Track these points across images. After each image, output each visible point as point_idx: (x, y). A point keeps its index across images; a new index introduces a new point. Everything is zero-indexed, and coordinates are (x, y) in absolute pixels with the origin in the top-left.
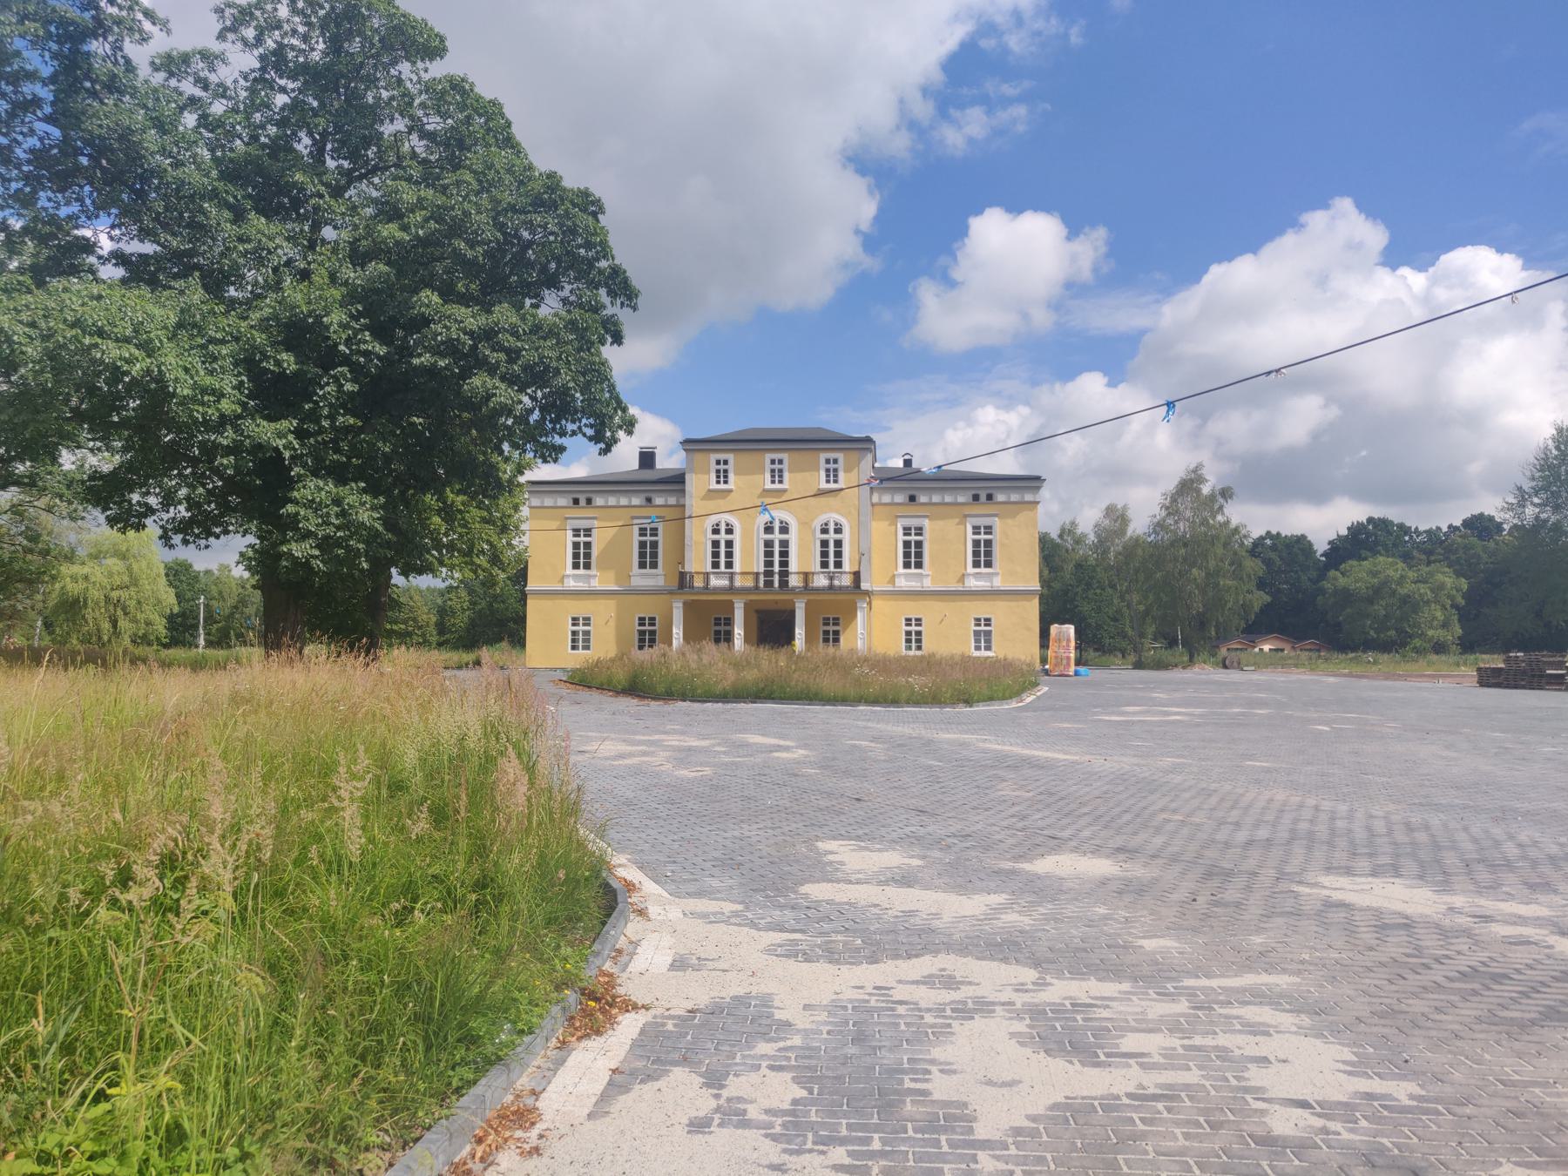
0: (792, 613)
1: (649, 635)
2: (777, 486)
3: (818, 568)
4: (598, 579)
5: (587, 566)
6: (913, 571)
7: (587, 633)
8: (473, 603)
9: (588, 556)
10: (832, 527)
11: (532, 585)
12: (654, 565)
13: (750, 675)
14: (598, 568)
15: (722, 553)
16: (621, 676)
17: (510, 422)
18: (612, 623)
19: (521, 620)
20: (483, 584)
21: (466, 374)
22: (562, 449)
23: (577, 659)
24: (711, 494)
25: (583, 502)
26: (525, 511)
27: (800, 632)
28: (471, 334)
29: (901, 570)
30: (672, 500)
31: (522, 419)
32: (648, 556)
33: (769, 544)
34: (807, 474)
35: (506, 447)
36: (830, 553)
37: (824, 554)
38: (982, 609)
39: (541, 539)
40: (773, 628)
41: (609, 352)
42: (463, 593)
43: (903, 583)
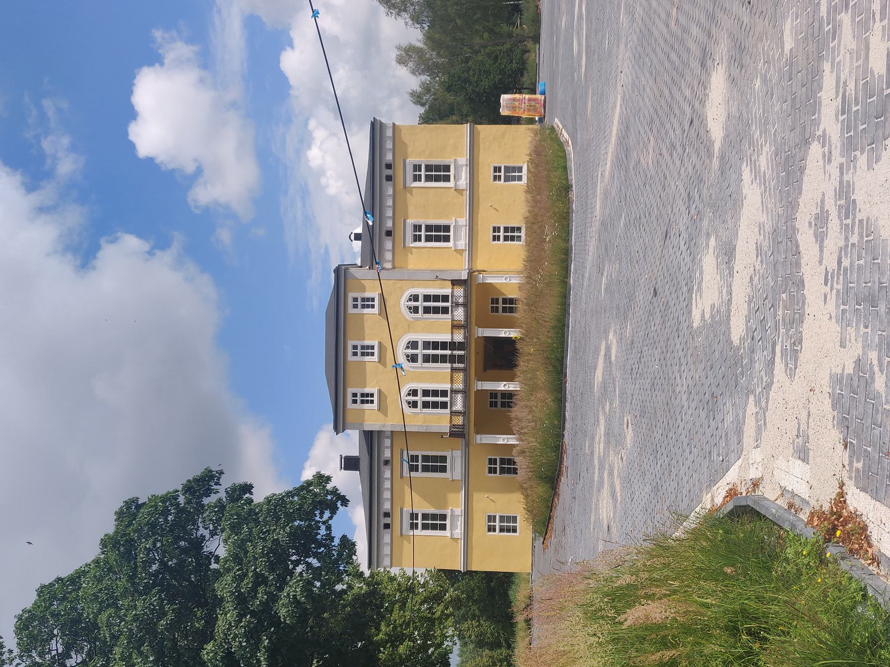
0: (488, 339)
1: (505, 465)
2: (376, 351)
3: (449, 316)
4: (455, 508)
5: (443, 517)
6: (451, 234)
7: (502, 519)
8: (474, 617)
9: (434, 517)
12: (444, 459)
13: (542, 377)
14: (445, 508)
15: (434, 400)
16: (541, 490)
17: (318, 584)
18: (493, 496)
19: (489, 576)
20: (459, 609)
21: (275, 620)
22: (344, 538)
23: (525, 528)
24: (382, 408)
25: (388, 520)
26: (395, 571)
27: (503, 333)
28: (241, 616)
29: (451, 244)
30: (387, 442)
31: (316, 573)
32: (436, 464)
33: (427, 359)
34: (366, 324)
35: (339, 587)
36: (434, 305)
37: (436, 310)
38: (486, 174)
39: (420, 557)
40: (500, 357)
41: (259, 496)
42: (465, 626)
43: (462, 243)
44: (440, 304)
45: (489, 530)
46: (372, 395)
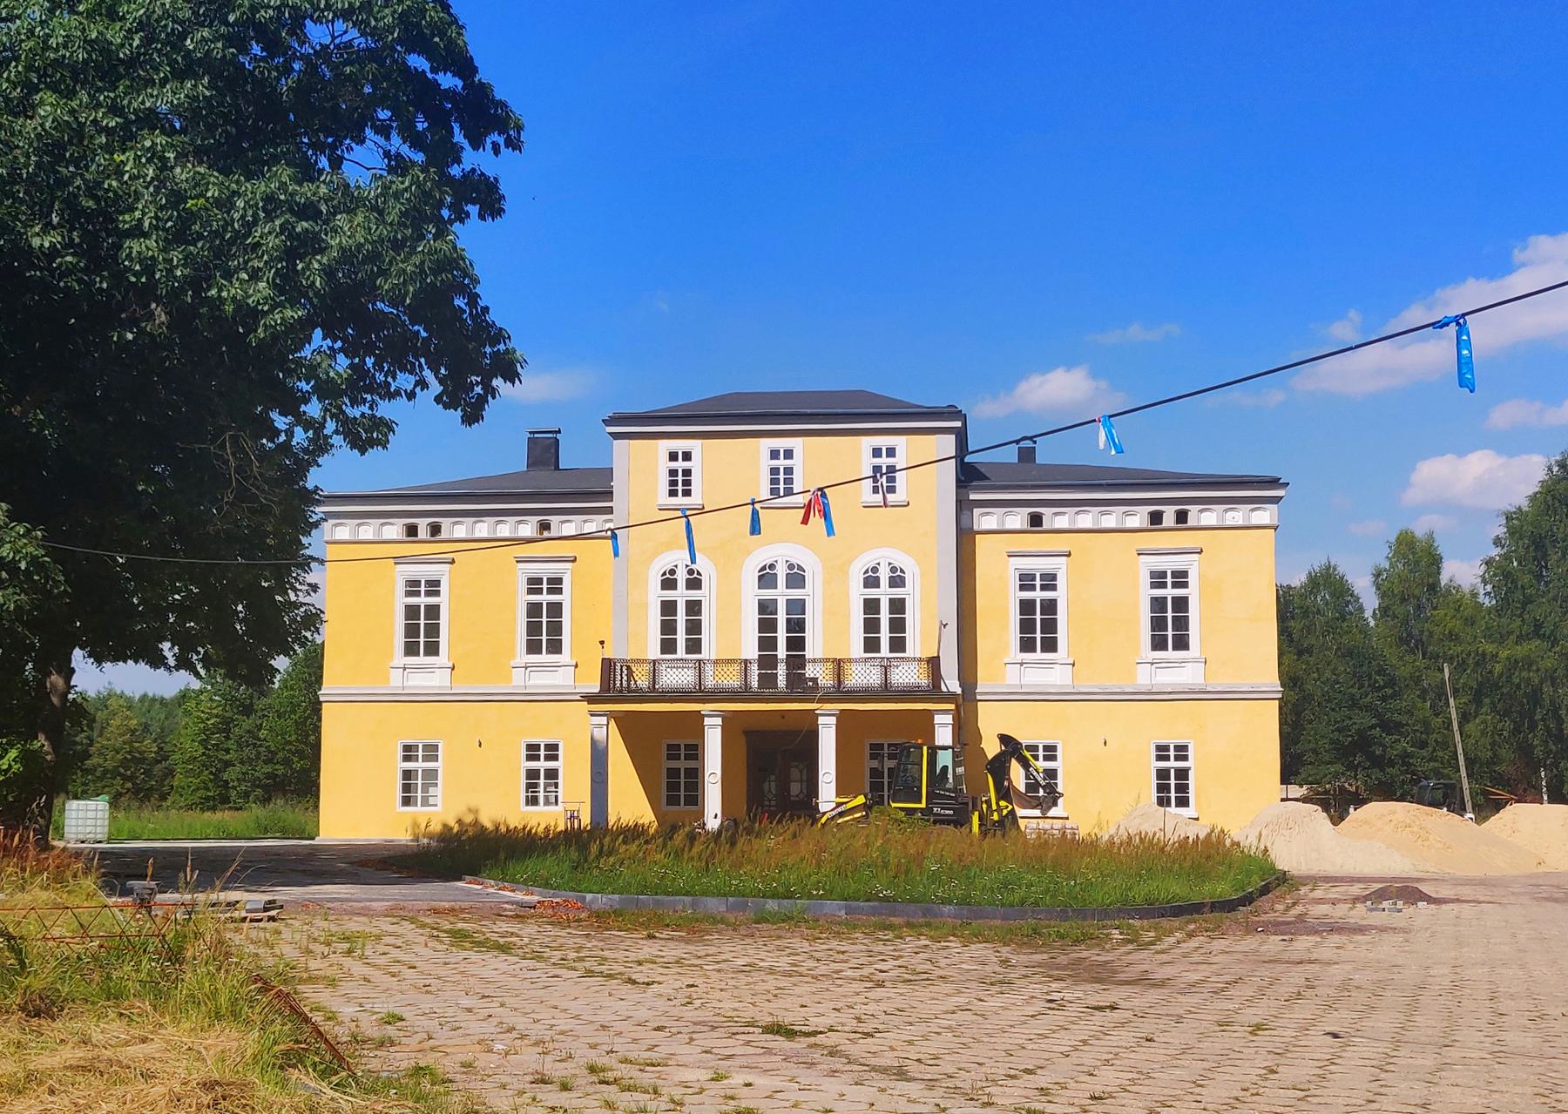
10: (884, 575)
11: (327, 688)
15: (682, 624)
44: (885, 635)
45: (407, 748)
46: (687, 493)
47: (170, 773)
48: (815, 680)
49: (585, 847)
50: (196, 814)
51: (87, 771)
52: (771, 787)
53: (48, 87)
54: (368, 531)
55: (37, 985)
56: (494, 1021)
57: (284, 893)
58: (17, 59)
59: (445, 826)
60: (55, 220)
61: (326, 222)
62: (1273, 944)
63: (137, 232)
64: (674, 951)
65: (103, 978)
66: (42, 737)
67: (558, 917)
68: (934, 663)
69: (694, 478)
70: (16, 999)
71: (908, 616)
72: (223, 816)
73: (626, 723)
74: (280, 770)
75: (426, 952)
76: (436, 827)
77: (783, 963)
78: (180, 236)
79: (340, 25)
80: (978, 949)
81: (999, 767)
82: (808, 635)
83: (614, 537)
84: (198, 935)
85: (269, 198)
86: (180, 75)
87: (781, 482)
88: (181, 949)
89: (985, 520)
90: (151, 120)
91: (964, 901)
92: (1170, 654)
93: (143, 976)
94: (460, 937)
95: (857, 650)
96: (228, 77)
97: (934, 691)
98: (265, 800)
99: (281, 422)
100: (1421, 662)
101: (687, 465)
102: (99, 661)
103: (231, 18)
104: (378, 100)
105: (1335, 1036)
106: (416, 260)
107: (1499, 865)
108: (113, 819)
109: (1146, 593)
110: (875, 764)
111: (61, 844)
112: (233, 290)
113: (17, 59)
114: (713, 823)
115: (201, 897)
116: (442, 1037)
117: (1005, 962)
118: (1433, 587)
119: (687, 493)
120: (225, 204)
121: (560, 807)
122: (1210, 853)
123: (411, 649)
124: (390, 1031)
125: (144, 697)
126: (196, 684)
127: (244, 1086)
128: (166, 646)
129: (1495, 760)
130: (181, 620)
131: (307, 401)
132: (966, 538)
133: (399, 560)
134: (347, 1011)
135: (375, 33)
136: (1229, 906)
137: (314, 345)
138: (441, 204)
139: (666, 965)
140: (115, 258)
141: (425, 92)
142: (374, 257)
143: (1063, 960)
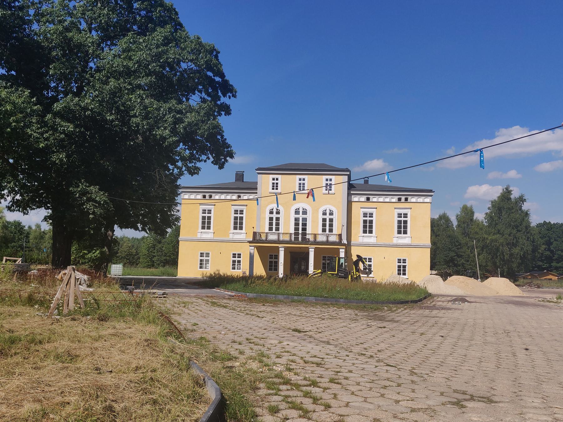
0: (308, 254)
10: (328, 212)
11: (181, 237)
15: (274, 223)
44: (327, 228)
45: (201, 254)
46: (277, 189)
47: (139, 258)
48: (309, 239)
49: (247, 281)
50: (145, 269)
51: (117, 257)
52: (296, 267)
53: (113, 77)
54: (193, 196)
55: (102, 312)
56: (222, 326)
57: (168, 291)
58: (105, 70)
59: (211, 274)
60: (113, 112)
61: (184, 115)
62: (427, 312)
63: (135, 116)
64: (269, 309)
65: (120, 311)
66: (106, 248)
67: (239, 299)
68: (340, 236)
69: (279, 185)
70: (96, 316)
71: (334, 223)
72: (153, 270)
73: (258, 248)
74: (168, 258)
75: (205, 307)
76: (208, 274)
77: (298, 313)
78: (146, 117)
79: (190, 64)
80: (349, 311)
81: (356, 263)
82: (307, 227)
83: (257, 200)
84: (145, 301)
85: (170, 108)
86: (147, 75)
87: (302, 187)
88: (141, 304)
89: (355, 199)
90: (139, 87)
91: (346, 298)
92: (402, 235)
93: (130, 311)
94: (214, 304)
95: (320, 231)
96: (160, 76)
97: (340, 243)
98: (164, 266)
99: (171, 167)
100: (468, 240)
101: (277, 181)
102: (121, 228)
103: (161, 61)
104: (198, 84)
105: (442, 337)
106: (208, 126)
107: (487, 293)
108: (124, 270)
109: (396, 219)
110: (324, 262)
111: (110, 276)
112: (159, 132)
113: (105, 70)
114: (281, 276)
115: (146, 291)
116: (208, 330)
117: (356, 315)
118: (472, 220)
119: (277, 189)
120: (158, 109)
121: (241, 270)
122: (411, 288)
123: (203, 228)
124: (195, 327)
125: (133, 238)
126: (146, 235)
127: (156, 341)
128: (139, 225)
129: (487, 265)
130: (143, 218)
131: (178, 162)
132: (350, 203)
133: (201, 204)
134: (184, 322)
135: (199, 66)
136: (416, 302)
137: (180, 147)
138: (215, 111)
139: (268, 313)
140: (129, 123)
141: (211, 82)
142: (197, 125)
143: (372, 314)
